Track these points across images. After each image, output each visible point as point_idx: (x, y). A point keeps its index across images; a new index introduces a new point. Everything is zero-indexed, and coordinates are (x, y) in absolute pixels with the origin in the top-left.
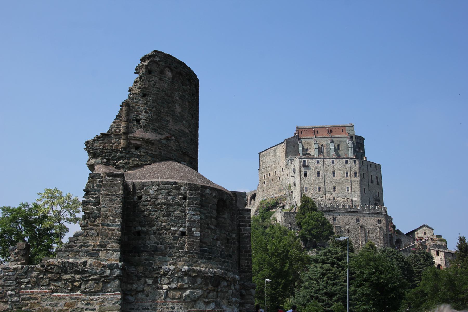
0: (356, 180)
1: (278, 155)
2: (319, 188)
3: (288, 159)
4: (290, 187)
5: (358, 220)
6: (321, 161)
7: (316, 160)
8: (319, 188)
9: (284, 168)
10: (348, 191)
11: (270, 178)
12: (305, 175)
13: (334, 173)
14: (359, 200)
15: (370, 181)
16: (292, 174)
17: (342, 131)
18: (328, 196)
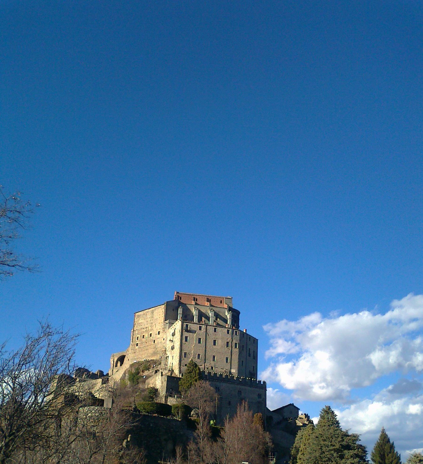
0: (236, 351)
1: (155, 317)
2: (199, 355)
3: (166, 322)
4: (165, 351)
5: (240, 392)
6: (203, 327)
7: (199, 326)
8: (199, 355)
9: (161, 331)
10: (227, 362)
11: (144, 340)
12: (186, 340)
13: (215, 341)
14: (237, 372)
15: (248, 355)
16: (170, 337)
17: (221, 303)
18: (207, 365)
